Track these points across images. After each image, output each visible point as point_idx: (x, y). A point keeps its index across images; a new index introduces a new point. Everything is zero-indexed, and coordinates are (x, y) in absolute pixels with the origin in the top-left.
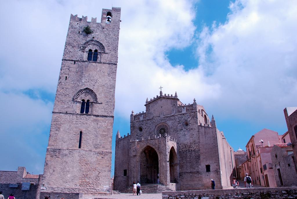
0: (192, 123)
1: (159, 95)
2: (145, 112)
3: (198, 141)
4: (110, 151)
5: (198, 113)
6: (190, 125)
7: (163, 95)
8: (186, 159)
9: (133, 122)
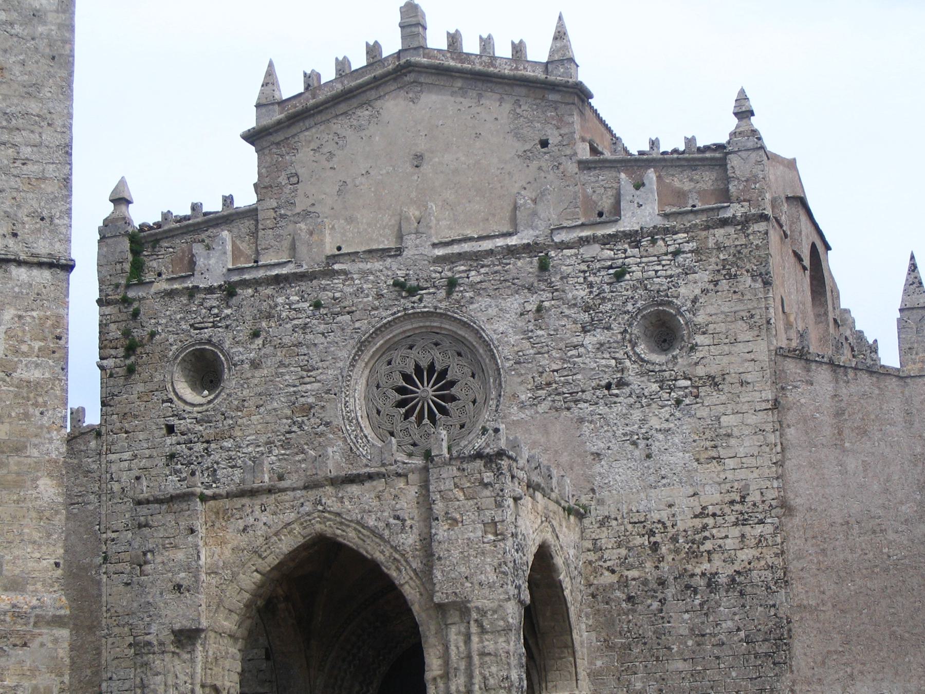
0: (721, 327)
1: (392, 44)
2: (246, 198)
3: (770, 495)
4: (47, 599)
5: (771, 232)
6: (699, 339)
7: (436, 40)
8: (652, 663)
9: (126, 301)
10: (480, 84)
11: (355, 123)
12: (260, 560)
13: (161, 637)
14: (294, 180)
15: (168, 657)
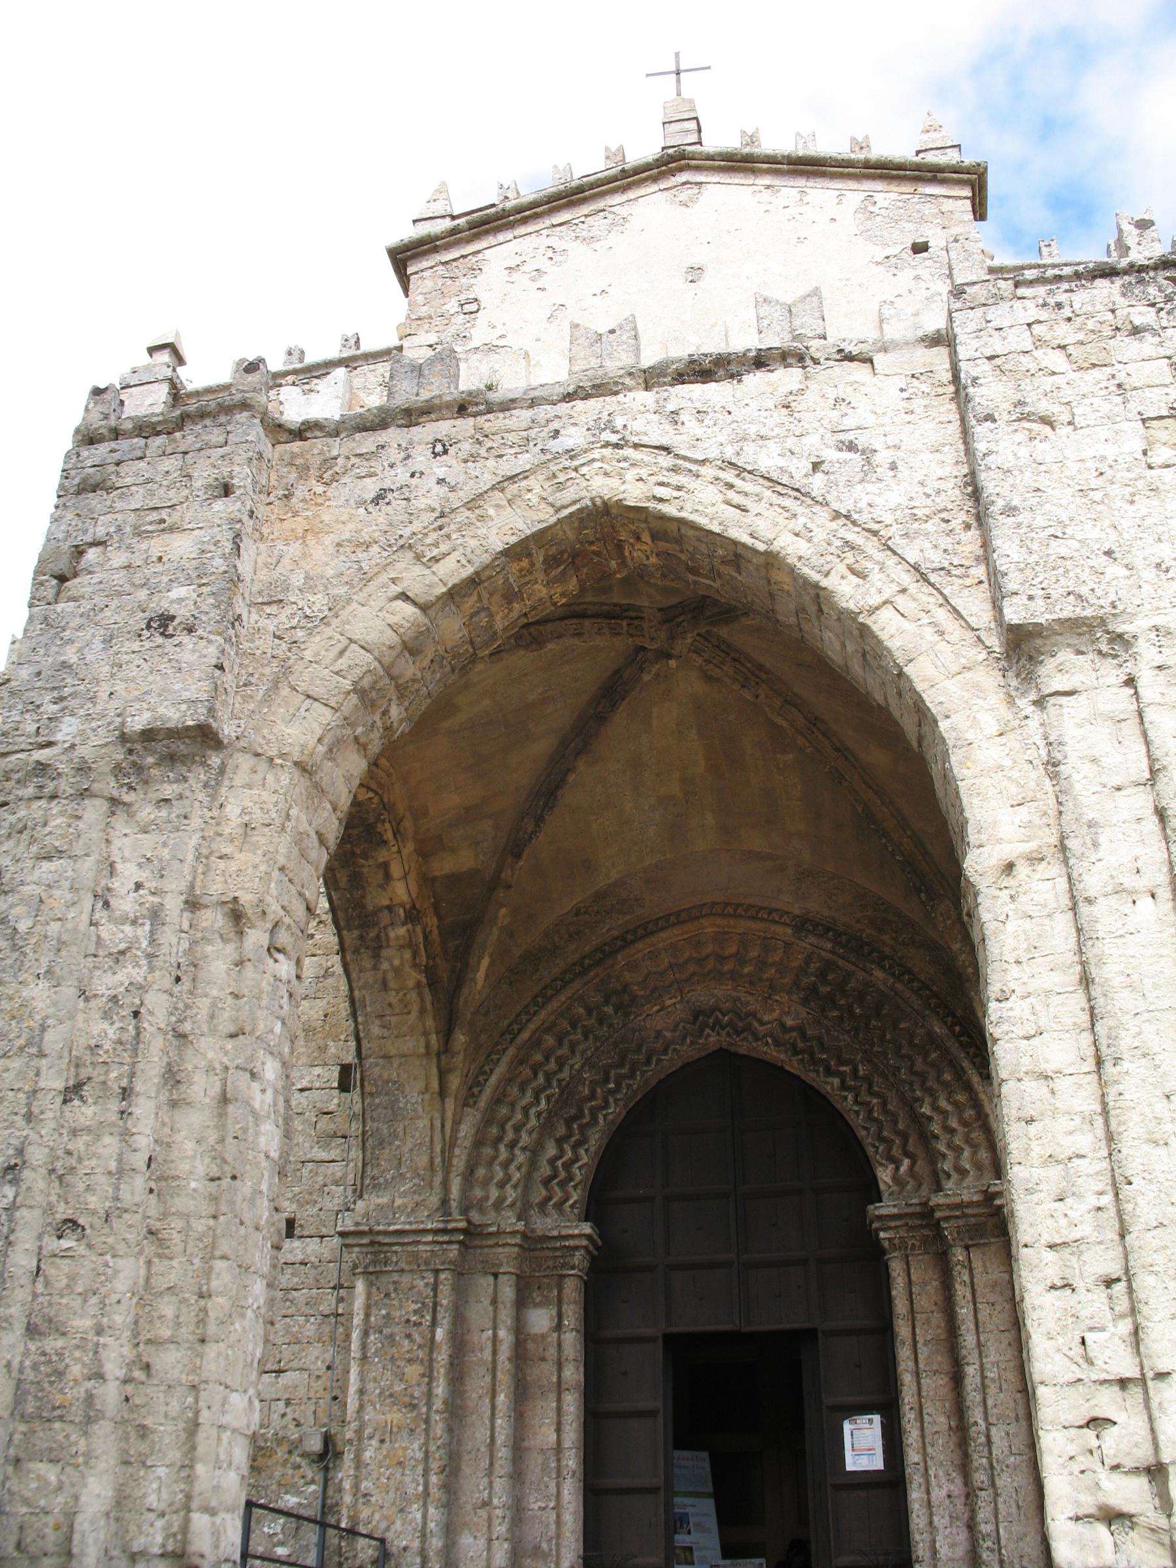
10: (801, 182)
11: (584, 234)
12: (418, 570)
13: (84, 751)
14: (473, 307)
15: (93, 811)
